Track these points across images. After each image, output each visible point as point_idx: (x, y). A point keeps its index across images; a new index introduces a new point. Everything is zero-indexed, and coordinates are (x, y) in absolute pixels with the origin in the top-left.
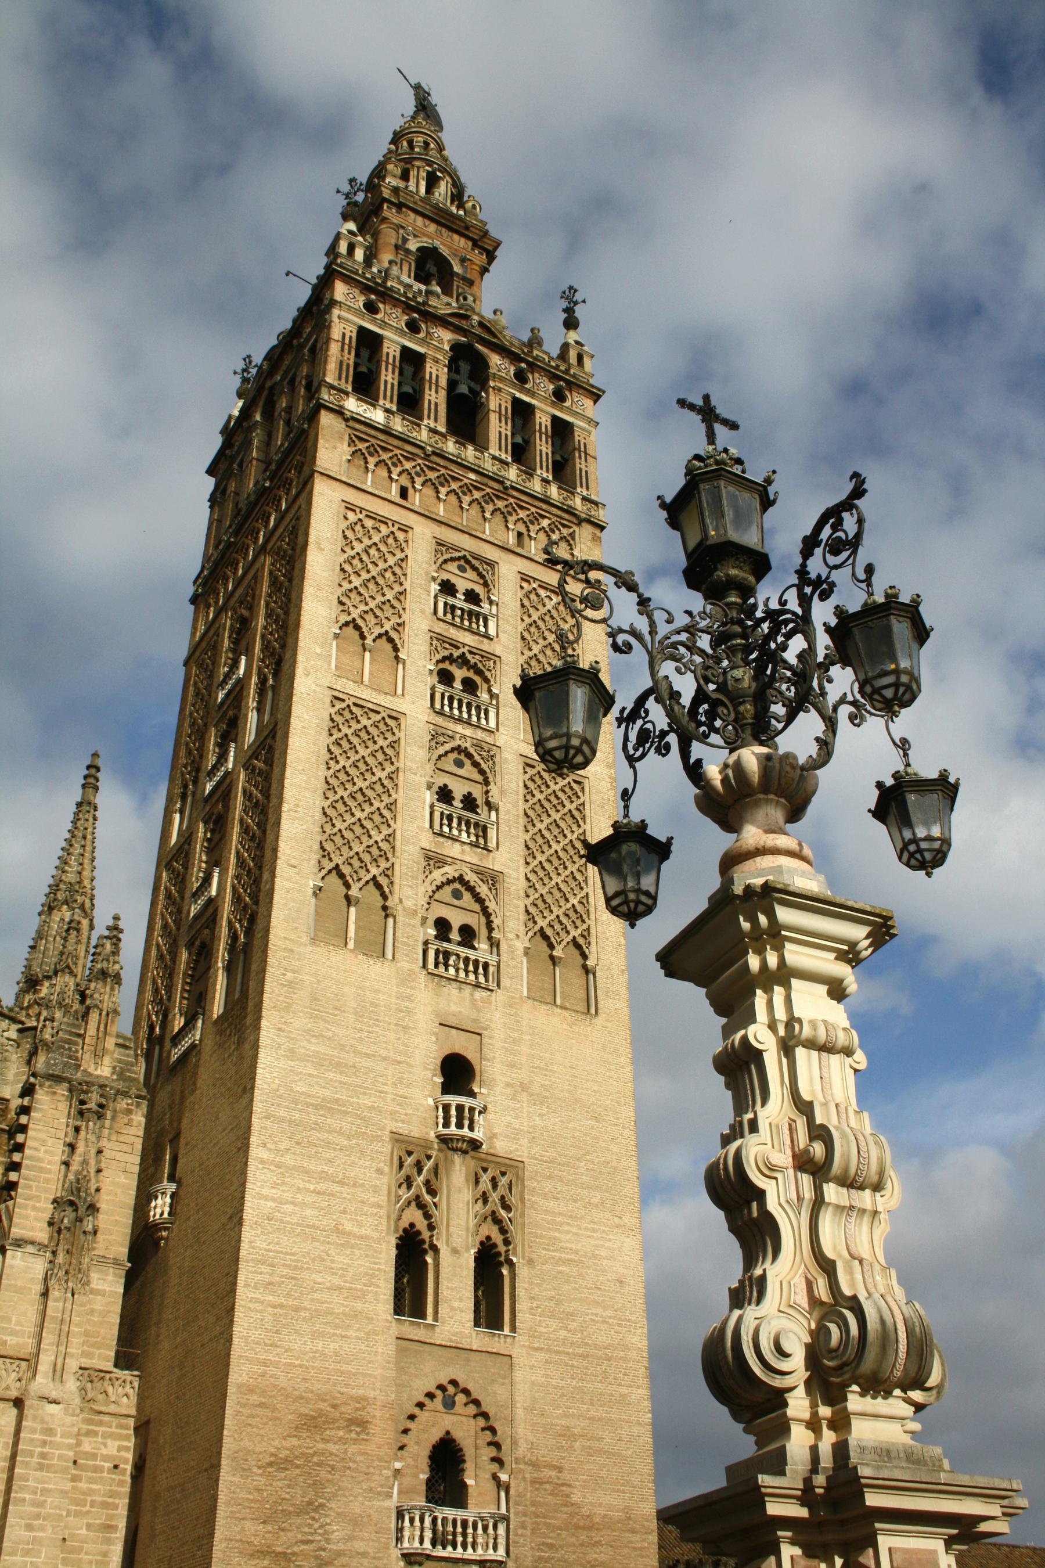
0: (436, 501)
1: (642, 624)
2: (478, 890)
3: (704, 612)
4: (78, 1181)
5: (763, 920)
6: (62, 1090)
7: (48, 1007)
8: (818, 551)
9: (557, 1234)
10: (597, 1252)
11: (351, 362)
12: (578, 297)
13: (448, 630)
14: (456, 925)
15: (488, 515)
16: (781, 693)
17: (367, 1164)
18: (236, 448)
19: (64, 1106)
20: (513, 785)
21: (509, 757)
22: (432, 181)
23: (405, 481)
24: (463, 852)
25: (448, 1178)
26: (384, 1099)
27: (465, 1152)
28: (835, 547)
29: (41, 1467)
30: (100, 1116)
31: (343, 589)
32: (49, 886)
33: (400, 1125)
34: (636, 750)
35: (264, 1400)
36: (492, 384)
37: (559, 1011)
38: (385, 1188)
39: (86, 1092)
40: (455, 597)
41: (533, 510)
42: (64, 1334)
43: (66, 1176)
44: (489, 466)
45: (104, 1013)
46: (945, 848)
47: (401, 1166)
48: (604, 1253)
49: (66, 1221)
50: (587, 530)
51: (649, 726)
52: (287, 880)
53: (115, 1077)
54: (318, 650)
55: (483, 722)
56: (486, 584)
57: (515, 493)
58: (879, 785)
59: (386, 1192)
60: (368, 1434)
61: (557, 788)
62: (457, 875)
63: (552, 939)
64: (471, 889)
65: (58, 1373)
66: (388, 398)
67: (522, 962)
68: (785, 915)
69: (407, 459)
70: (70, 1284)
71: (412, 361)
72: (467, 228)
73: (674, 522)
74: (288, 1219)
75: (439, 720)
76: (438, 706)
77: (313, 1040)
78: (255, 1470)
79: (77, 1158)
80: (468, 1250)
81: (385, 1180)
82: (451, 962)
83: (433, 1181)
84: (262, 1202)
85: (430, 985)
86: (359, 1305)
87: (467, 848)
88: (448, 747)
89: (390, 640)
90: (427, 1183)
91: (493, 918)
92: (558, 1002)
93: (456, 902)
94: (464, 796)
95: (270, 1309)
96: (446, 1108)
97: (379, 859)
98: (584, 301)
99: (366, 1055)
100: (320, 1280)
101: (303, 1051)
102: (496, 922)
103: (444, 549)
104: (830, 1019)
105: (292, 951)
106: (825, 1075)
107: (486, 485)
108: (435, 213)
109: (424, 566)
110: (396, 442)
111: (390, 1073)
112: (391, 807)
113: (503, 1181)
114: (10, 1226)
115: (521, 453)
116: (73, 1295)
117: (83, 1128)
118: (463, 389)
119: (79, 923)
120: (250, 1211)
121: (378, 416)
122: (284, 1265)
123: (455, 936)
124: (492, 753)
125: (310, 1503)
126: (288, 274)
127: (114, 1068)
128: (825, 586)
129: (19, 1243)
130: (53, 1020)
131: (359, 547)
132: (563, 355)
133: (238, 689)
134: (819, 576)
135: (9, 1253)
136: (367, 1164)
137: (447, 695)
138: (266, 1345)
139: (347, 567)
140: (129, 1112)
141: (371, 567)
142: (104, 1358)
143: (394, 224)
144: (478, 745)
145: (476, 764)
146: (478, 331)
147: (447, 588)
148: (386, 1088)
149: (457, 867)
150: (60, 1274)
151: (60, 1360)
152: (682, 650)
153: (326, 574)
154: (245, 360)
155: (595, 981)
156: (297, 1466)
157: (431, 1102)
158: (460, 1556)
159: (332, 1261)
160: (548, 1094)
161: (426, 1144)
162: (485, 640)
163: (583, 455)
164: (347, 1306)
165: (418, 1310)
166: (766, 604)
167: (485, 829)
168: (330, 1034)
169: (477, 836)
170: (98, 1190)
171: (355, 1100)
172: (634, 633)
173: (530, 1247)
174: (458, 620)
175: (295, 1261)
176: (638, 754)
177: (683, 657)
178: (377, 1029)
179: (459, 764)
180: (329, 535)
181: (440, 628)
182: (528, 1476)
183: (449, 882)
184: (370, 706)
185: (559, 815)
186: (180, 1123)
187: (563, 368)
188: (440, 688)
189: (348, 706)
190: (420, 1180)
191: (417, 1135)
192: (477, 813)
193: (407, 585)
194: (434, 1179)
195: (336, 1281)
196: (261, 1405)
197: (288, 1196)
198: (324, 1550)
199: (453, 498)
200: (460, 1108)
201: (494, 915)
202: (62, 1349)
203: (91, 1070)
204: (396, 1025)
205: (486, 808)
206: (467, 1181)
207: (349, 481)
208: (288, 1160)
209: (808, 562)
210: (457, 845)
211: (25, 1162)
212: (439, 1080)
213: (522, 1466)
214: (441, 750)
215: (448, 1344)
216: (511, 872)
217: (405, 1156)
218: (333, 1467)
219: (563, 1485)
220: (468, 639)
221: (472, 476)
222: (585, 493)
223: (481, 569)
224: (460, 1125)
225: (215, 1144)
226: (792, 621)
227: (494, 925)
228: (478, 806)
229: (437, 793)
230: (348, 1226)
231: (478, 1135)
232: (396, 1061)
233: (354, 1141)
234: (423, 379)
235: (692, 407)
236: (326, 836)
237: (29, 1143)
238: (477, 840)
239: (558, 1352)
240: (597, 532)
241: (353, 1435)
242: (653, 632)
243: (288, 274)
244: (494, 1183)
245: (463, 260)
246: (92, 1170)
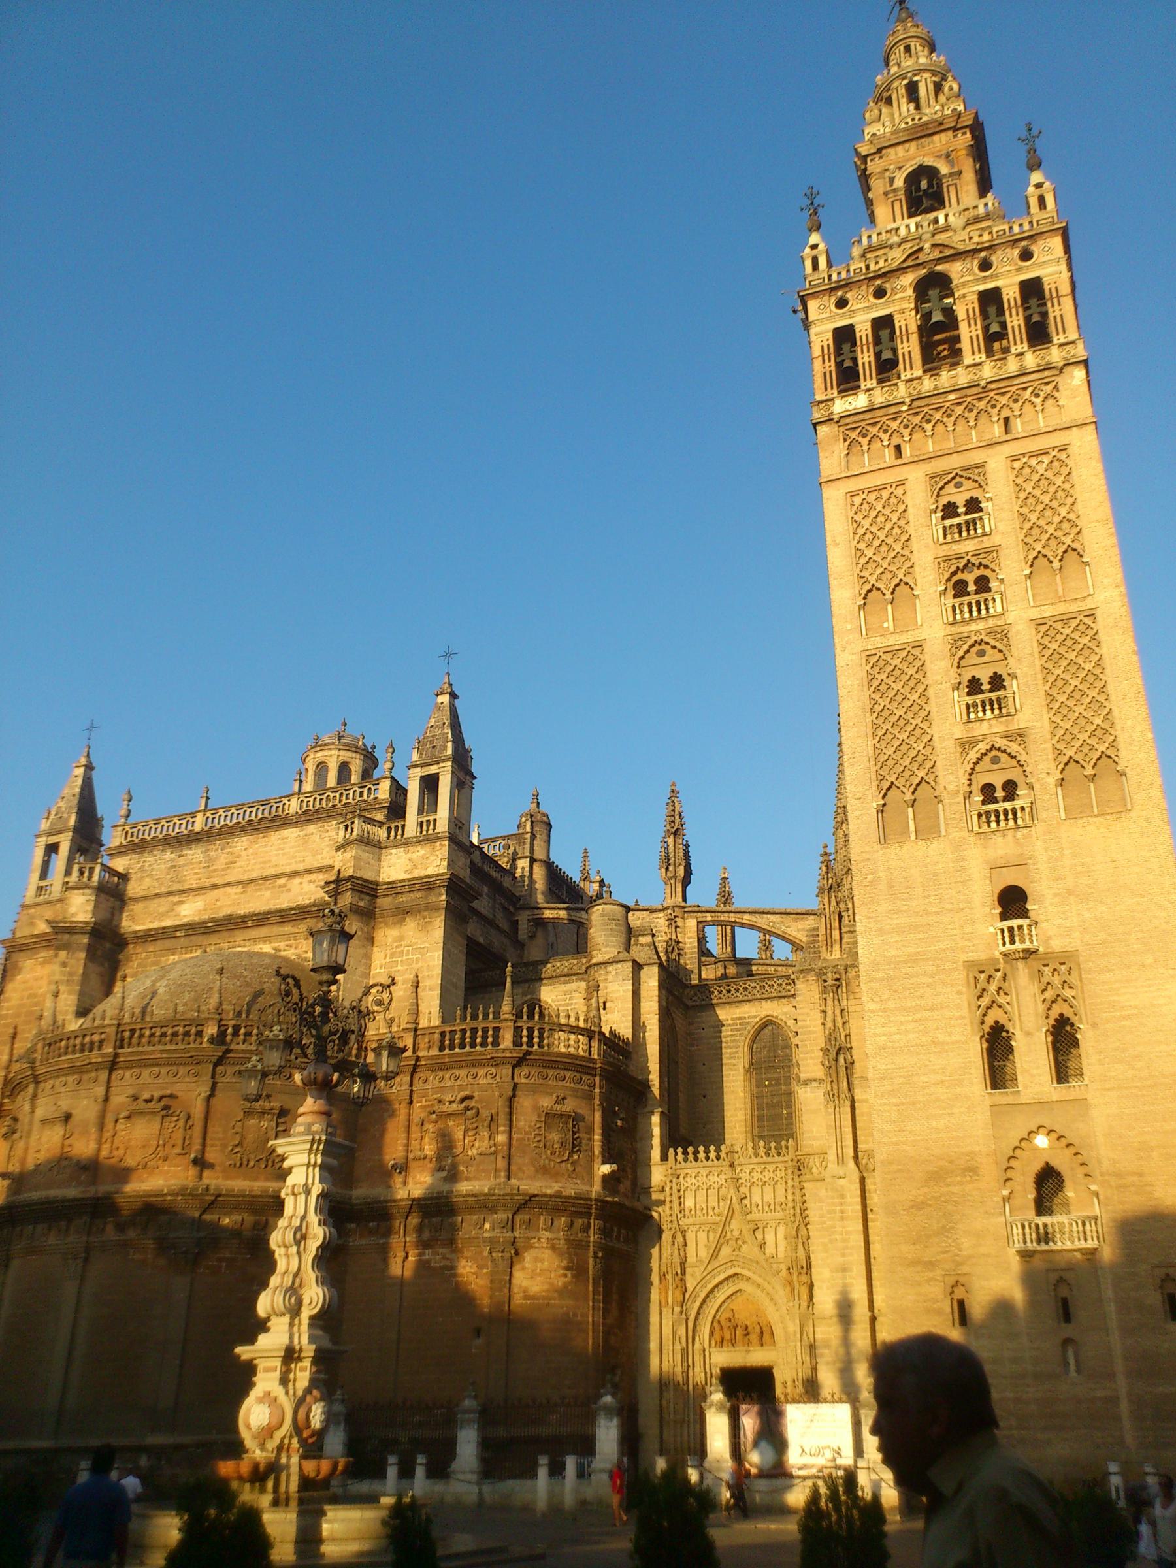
6: (812, 977)
9: (1116, 998)
10: (1155, 1002)
14: (998, 785)
21: (1020, 627)
24: (990, 725)
25: (1014, 979)
29: (842, 1219)
33: (970, 954)
38: (965, 1004)
42: (838, 1134)
48: (1161, 1001)
57: (993, 386)
60: (978, 1175)
62: (989, 747)
71: (883, 325)
72: (941, 124)
74: (897, 1045)
78: (902, 1212)
81: (964, 997)
83: (1005, 986)
85: (979, 842)
86: (959, 1090)
87: (994, 722)
88: (965, 647)
93: (995, 767)
94: (991, 677)
95: (895, 1108)
96: (1002, 931)
99: (937, 913)
100: (926, 1080)
102: (1028, 769)
103: (937, 479)
107: (966, 396)
108: (912, 134)
120: (870, 1047)
122: (901, 1076)
123: (1000, 793)
125: (944, 1227)
144: (992, 632)
145: (994, 647)
146: (936, 254)
149: (988, 741)
156: (930, 1205)
157: (992, 929)
158: (1059, 1248)
160: (1092, 890)
162: (985, 538)
168: (906, 907)
171: (933, 948)
173: (1092, 1014)
178: (941, 891)
182: (1112, 1183)
184: (897, 648)
193: (911, 529)
195: (939, 1077)
196: (899, 1171)
197: (894, 1029)
198: (958, 1255)
200: (1011, 929)
208: (891, 1005)
210: (985, 724)
212: (998, 910)
213: (1107, 1178)
214: (961, 653)
216: (1035, 724)
218: (956, 1202)
219: (1146, 1185)
221: (952, 396)
224: (1013, 942)
239: (1126, 1088)
241: (969, 1179)
246: (839, 1024)
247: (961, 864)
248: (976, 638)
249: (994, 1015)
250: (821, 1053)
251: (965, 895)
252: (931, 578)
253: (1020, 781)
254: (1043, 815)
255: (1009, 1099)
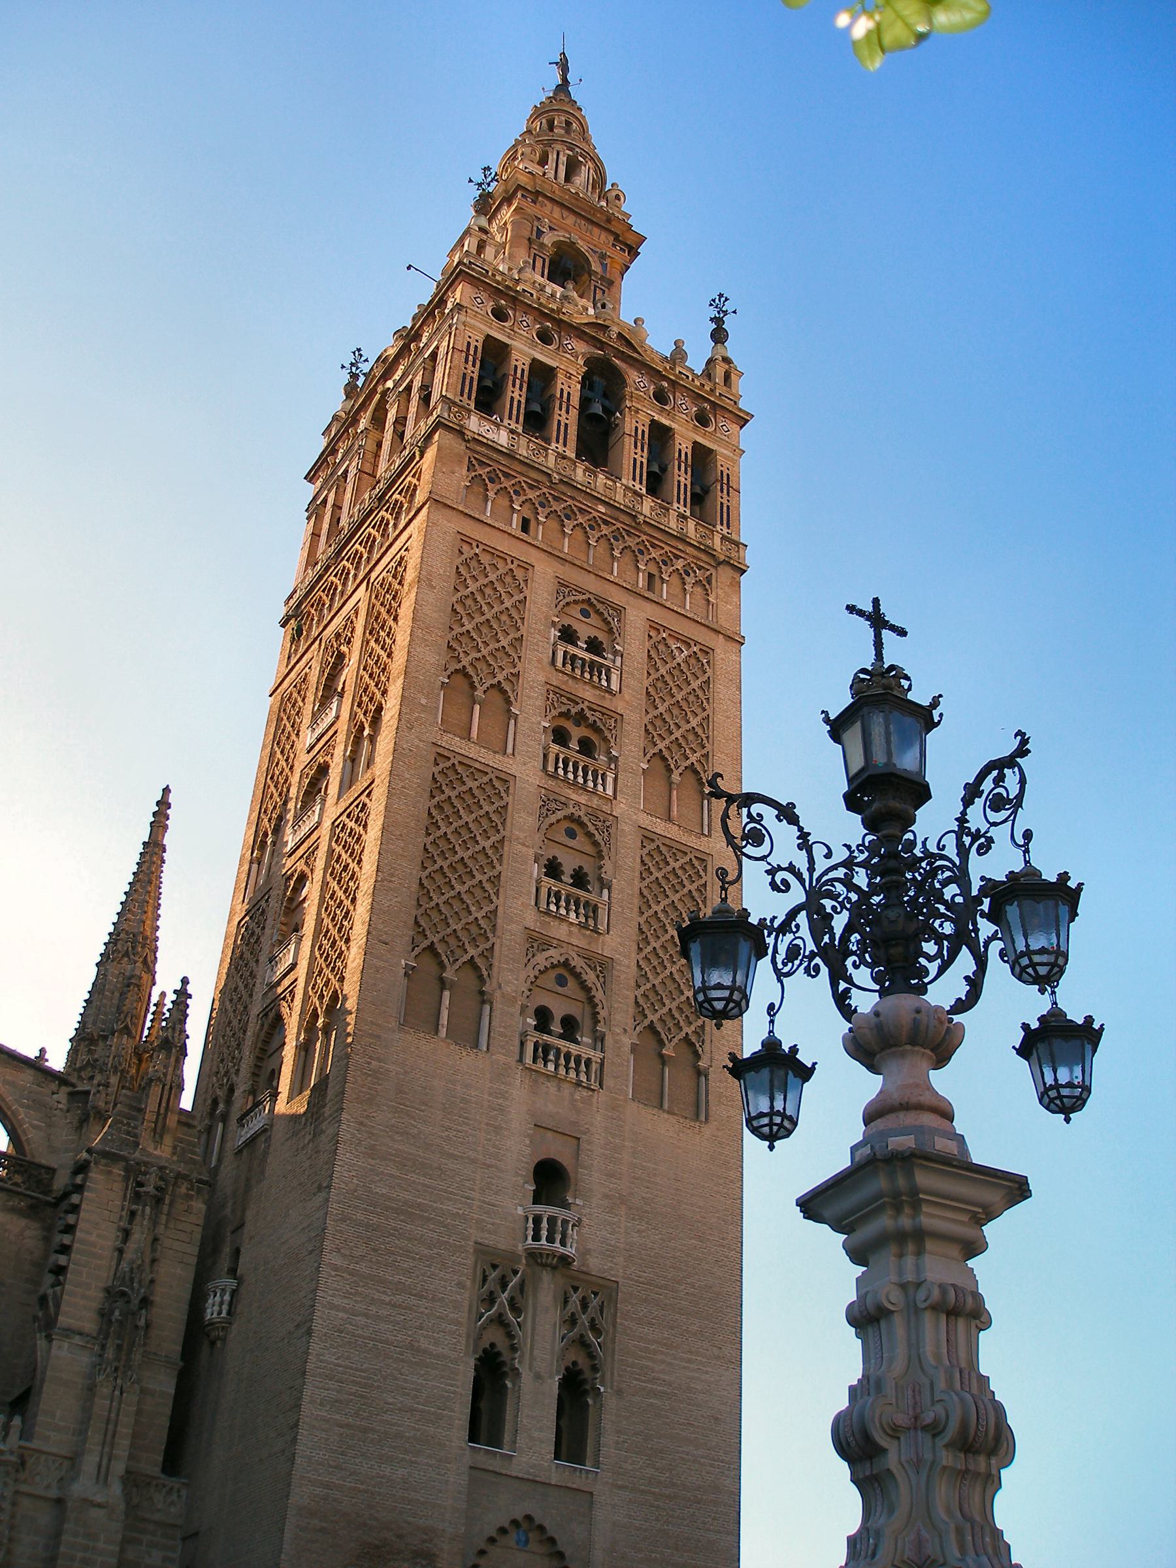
0: (560, 536)
1: (802, 864)
2: (584, 976)
3: (863, 845)
4: (132, 1270)
5: (901, 1182)
7: (101, 1071)
8: (979, 802)
11: (476, 376)
12: (728, 307)
13: (566, 683)
14: (558, 1014)
15: (616, 553)
16: (934, 930)
17: (448, 1276)
18: (340, 456)
19: (118, 1186)
20: (629, 861)
22: (572, 168)
23: (528, 514)
26: (471, 1207)
27: (554, 1268)
28: (997, 803)
30: (159, 1201)
31: (454, 633)
32: (110, 934)
34: (785, 964)
35: (324, 1525)
36: (628, 404)
37: (666, 1115)
38: (466, 1303)
39: (145, 1173)
40: (577, 646)
41: (667, 548)
43: (118, 1264)
44: (619, 497)
45: (167, 1087)
46: (1084, 1096)
47: (485, 1279)
49: (117, 1313)
50: (725, 573)
51: (799, 942)
52: (377, 958)
53: (175, 1158)
54: (423, 701)
55: (600, 788)
56: (610, 631)
58: (1025, 1027)
59: (466, 1309)
61: (677, 865)
63: (663, 1036)
64: (578, 976)
65: (102, 1476)
66: (514, 417)
67: (628, 1061)
68: (923, 1179)
69: (531, 487)
70: (119, 1381)
71: (541, 375)
72: (609, 221)
73: (836, 735)
75: (551, 783)
76: (551, 768)
77: (397, 1137)
79: (131, 1246)
80: (552, 1377)
81: (467, 1295)
82: (551, 1057)
83: (518, 1298)
84: (333, 1312)
87: (574, 929)
88: (560, 815)
89: (504, 692)
90: (512, 1301)
91: (599, 1009)
92: (666, 1106)
93: (560, 989)
96: (537, 1220)
97: (478, 939)
98: (734, 312)
100: (391, 1400)
101: (384, 1148)
102: (603, 1014)
104: (959, 1283)
105: (379, 1037)
106: (952, 1338)
109: (544, 609)
110: (519, 468)
111: (478, 1177)
112: (496, 880)
113: (594, 1302)
114: (57, 1315)
115: (655, 483)
116: (121, 1393)
117: (139, 1212)
118: (597, 409)
119: (140, 978)
121: (502, 438)
123: (556, 1027)
124: (608, 824)
126: (409, 268)
127: (175, 1148)
128: (983, 840)
129: (69, 1332)
130: (107, 1085)
131: (473, 587)
132: (708, 374)
133: (330, 733)
134: (978, 830)
135: (54, 1342)
136: (448, 1276)
137: (562, 756)
138: (330, 1466)
139: (459, 608)
140: (189, 1197)
141: (485, 608)
142: (152, 1462)
143: (529, 215)
144: (594, 814)
145: (590, 835)
147: (568, 635)
148: (473, 1194)
149: (563, 951)
150: (108, 1370)
151: (105, 1462)
152: (839, 888)
153: (435, 615)
154: (354, 353)
155: (707, 1085)
157: (520, 1211)
159: (405, 1381)
160: (647, 1208)
161: (513, 1257)
163: (725, 487)
164: (418, 1430)
165: (495, 1440)
166: (924, 843)
167: (595, 909)
168: (416, 1131)
169: (587, 917)
170: (152, 1281)
172: (791, 869)
173: (619, 1376)
174: (578, 672)
175: (364, 1378)
176: (786, 970)
177: (840, 895)
179: (571, 834)
180: (441, 572)
181: (557, 679)
183: (553, 966)
184: (477, 765)
185: (678, 896)
186: (244, 1211)
187: (707, 388)
188: (555, 748)
189: (454, 764)
190: (504, 1296)
191: (503, 1247)
192: (588, 891)
194: (520, 1296)
199: (579, 533)
200: (552, 1221)
201: (600, 1006)
202: (106, 1449)
203: (150, 1149)
204: (487, 1124)
205: (597, 885)
206: (555, 1298)
207: (467, 511)
208: (363, 1268)
209: (968, 810)
210: (564, 927)
211: (76, 1245)
214: (553, 818)
215: (526, 1476)
217: (489, 1270)
220: (588, 694)
221: (602, 509)
222: (725, 531)
223: (606, 615)
224: (550, 1239)
225: (284, 1243)
226: (949, 869)
227: (600, 1017)
228: (589, 882)
229: (545, 866)
230: (424, 1344)
231: (570, 1251)
232: (485, 1164)
233: (435, 1251)
234: (553, 396)
235: (861, 613)
236: (422, 910)
237: (81, 1225)
238: (586, 920)
239: (643, 1492)
240: (736, 575)
242: (811, 869)
243: (409, 268)
244: (584, 1304)
245: (603, 256)
246: (147, 1261)
247: (500, 1101)
248: (573, 811)
249: (495, 1336)
250: (101, 1295)
251: (494, 1146)
252: (538, 703)
253: (586, 1024)
254: (608, 1081)
255: (495, 1464)
